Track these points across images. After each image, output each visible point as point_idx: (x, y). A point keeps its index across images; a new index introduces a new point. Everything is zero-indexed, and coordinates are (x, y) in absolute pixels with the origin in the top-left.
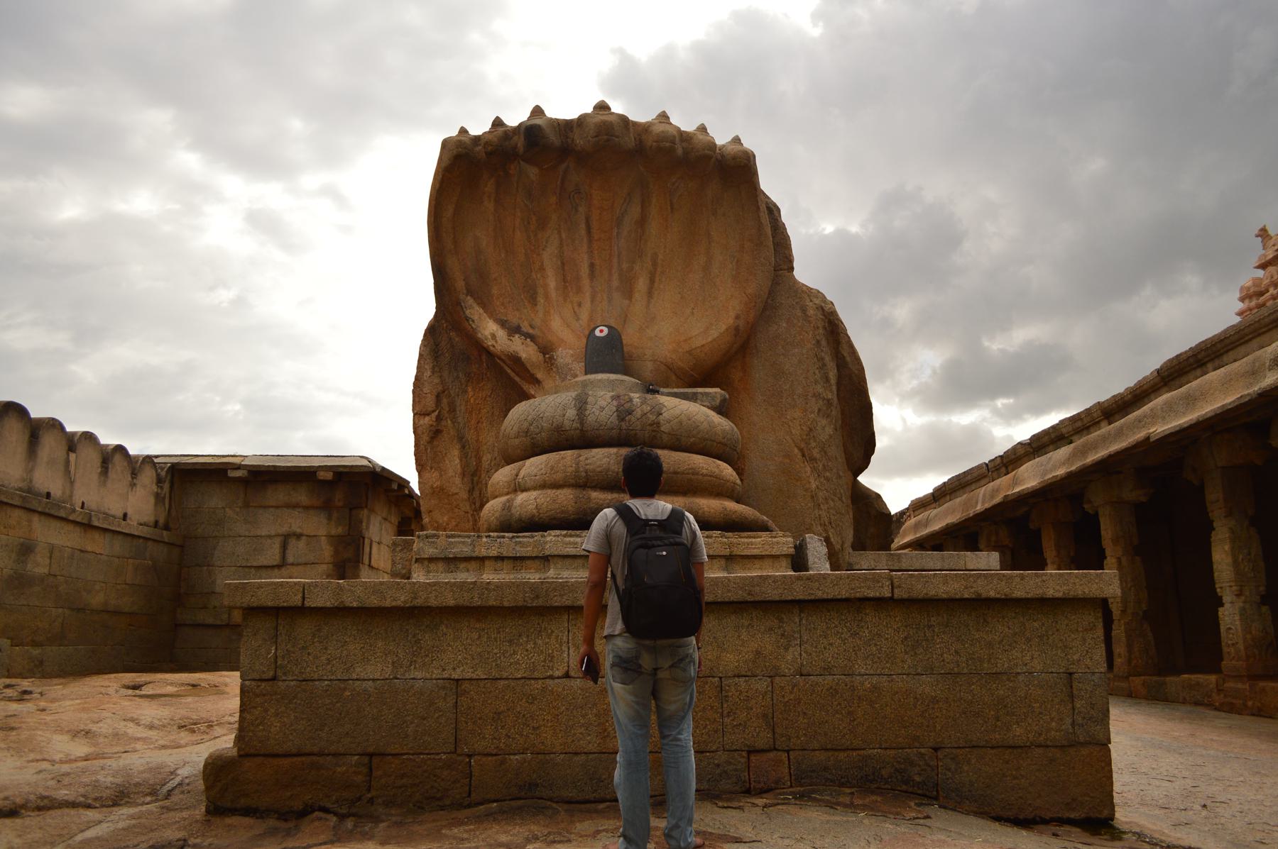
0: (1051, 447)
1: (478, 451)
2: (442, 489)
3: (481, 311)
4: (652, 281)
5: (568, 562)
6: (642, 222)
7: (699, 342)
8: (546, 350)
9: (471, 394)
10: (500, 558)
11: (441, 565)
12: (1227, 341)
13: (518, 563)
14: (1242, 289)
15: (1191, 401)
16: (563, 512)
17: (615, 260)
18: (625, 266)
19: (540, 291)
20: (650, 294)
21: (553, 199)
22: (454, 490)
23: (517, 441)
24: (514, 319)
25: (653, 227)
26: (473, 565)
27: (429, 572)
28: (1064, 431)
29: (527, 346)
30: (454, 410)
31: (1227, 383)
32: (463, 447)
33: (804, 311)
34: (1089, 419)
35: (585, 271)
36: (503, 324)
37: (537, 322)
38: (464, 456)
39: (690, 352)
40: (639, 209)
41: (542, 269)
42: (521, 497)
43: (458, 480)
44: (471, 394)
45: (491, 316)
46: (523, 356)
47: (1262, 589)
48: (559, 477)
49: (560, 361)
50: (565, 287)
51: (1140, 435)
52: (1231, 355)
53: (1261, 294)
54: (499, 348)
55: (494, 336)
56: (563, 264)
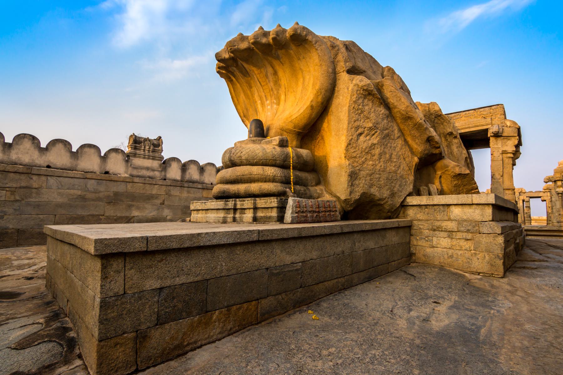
4: (286, 95)
6: (275, 73)
7: (294, 117)
10: (203, 210)
39: (291, 122)
40: (271, 69)
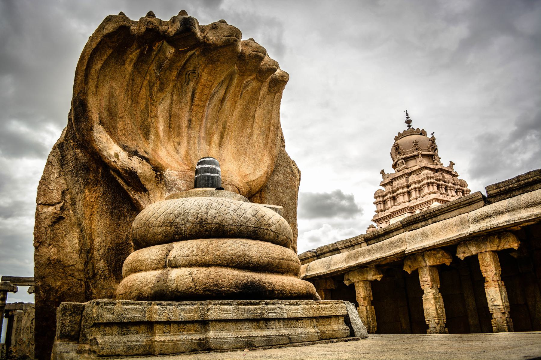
0: (328, 254)
1: (91, 235)
2: (59, 261)
3: (109, 137)
4: (222, 138)
5: (221, 325)
7: (252, 178)
8: (158, 169)
9: (87, 194)
10: (168, 323)
11: (115, 329)
12: (442, 210)
13: (182, 326)
14: (376, 193)
15: (424, 236)
16: (215, 285)
17: (204, 120)
18: (209, 125)
19: (153, 131)
20: (220, 144)
21: (175, 73)
22: (71, 262)
23: (160, 230)
24: (133, 146)
25: (227, 105)
26: (143, 328)
27: (105, 335)
28: (339, 247)
29: (143, 164)
30: (75, 204)
31: (446, 228)
32: (81, 231)
33: (292, 170)
34: (355, 242)
35: (184, 124)
36: (124, 148)
37: (149, 150)
38: (81, 238)
39: (247, 183)
40: (223, 92)
41: (156, 116)
42: (174, 273)
43: (75, 256)
44: (87, 194)
45: (115, 141)
46: (139, 171)
47: (445, 320)
48: (209, 258)
49: (168, 177)
50: (170, 131)
51: (398, 250)
52: (442, 217)
53: (383, 196)
54: (119, 164)
55: (117, 155)
56: (170, 116)
